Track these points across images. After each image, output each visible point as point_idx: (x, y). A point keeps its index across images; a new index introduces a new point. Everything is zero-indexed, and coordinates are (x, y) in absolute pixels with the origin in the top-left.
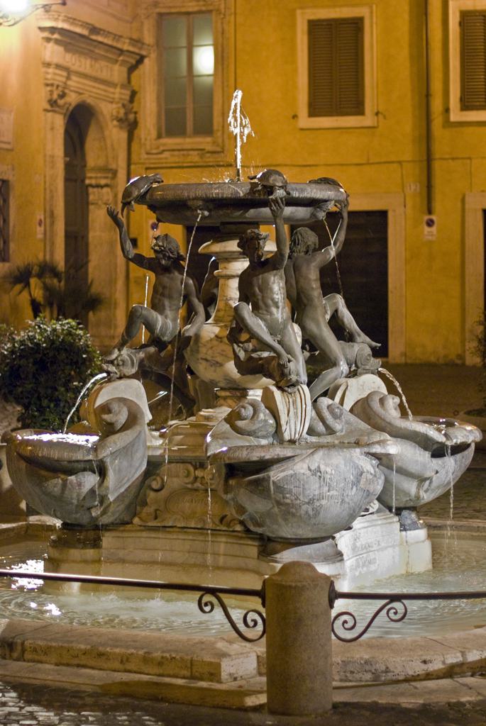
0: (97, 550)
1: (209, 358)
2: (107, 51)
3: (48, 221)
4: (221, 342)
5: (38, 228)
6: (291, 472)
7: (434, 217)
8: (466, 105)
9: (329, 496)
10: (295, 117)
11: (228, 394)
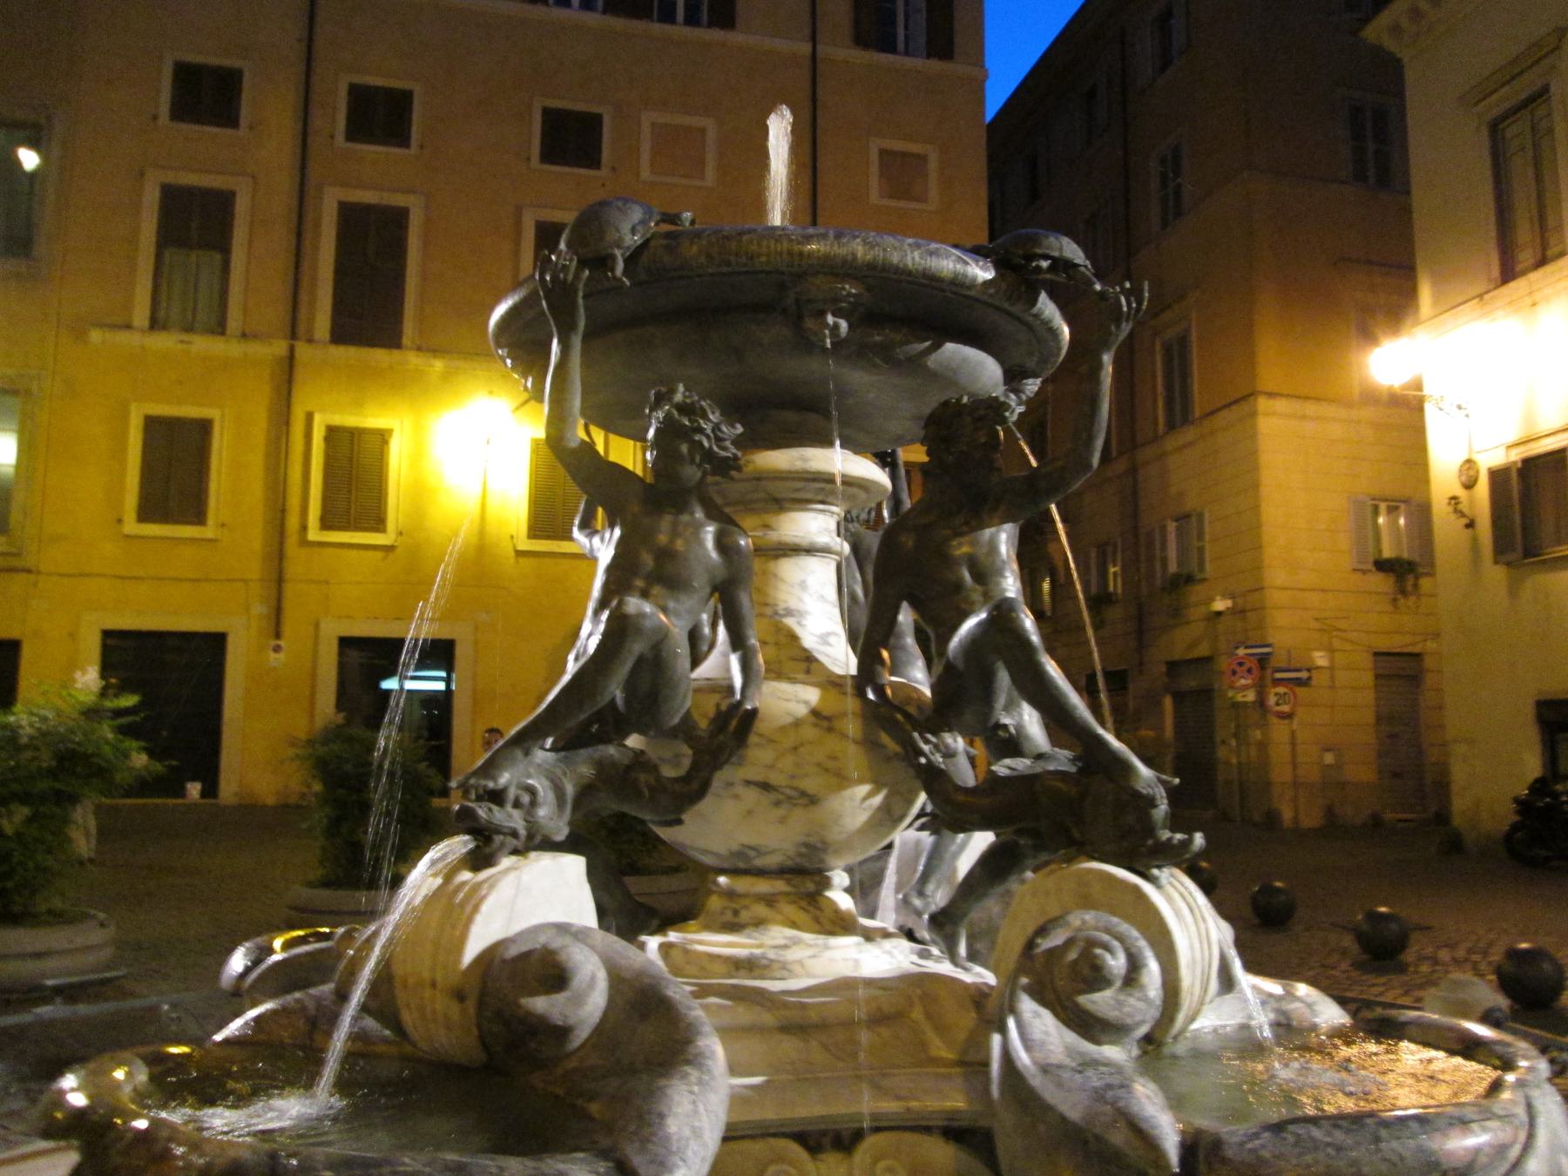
1: (776, 779)
4: (830, 730)
7: (282, 643)
8: (326, 524)
10: (120, 521)
11: (780, 885)
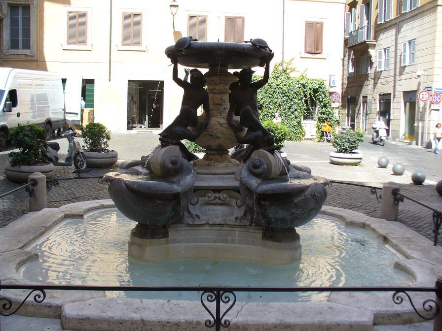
0: (166, 239)
1: (213, 134)
4: (222, 126)
6: (304, 197)
11: (216, 152)
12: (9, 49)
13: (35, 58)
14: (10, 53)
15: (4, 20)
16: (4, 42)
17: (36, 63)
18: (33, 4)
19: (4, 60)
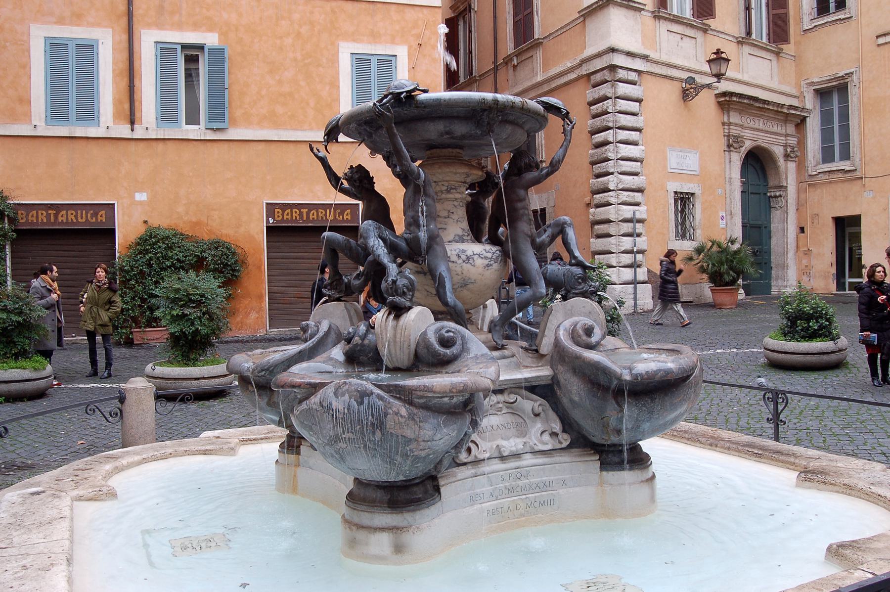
2: (775, 115)
3: (729, 217)
5: (721, 221)
9: (345, 438)
12: (818, 164)
13: (858, 174)
14: (818, 171)
15: (808, 119)
16: (809, 154)
17: (859, 182)
18: (852, 80)
19: (809, 185)
